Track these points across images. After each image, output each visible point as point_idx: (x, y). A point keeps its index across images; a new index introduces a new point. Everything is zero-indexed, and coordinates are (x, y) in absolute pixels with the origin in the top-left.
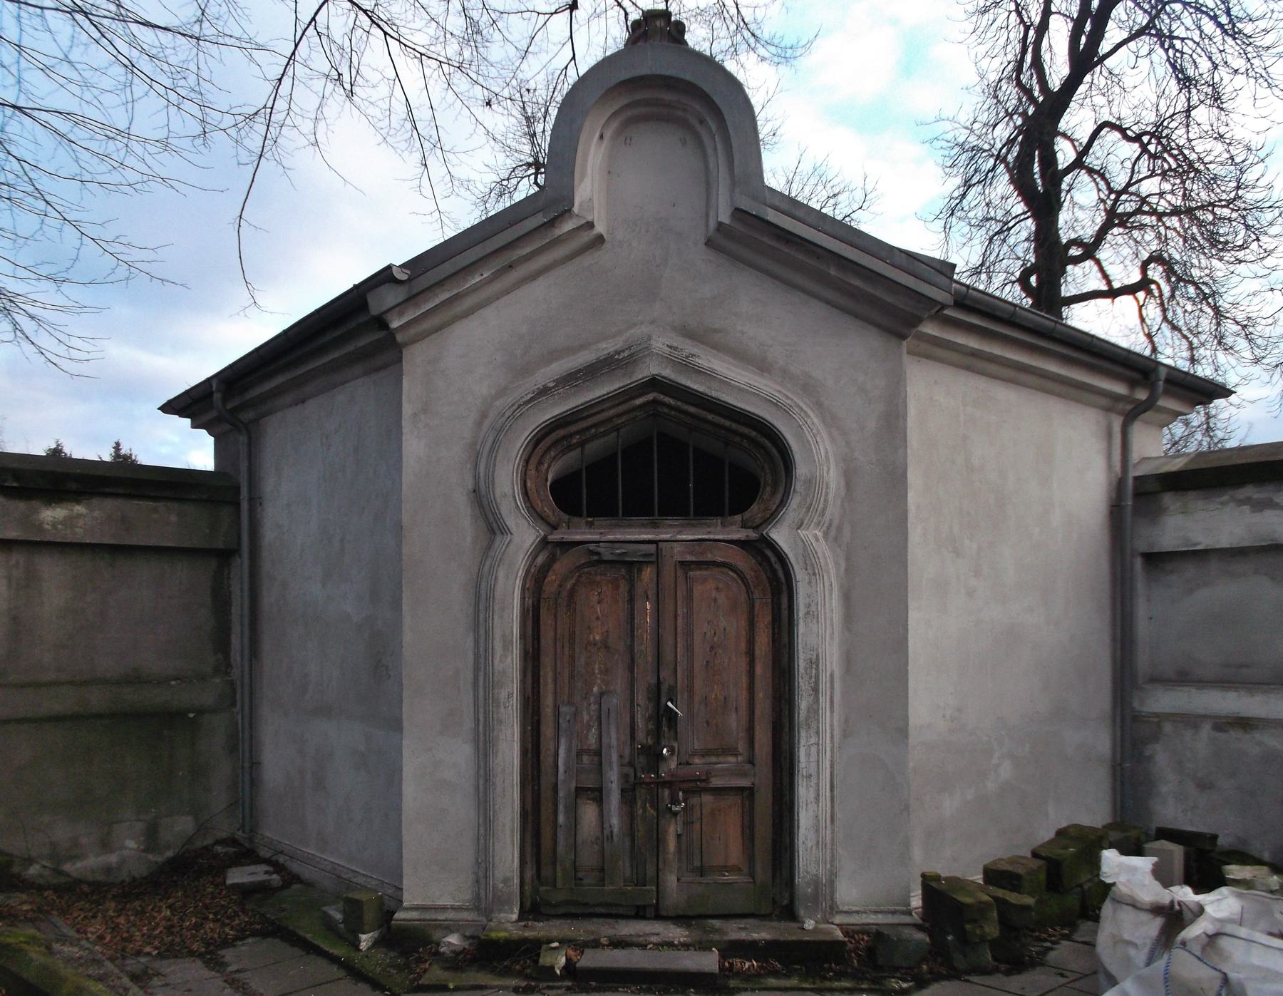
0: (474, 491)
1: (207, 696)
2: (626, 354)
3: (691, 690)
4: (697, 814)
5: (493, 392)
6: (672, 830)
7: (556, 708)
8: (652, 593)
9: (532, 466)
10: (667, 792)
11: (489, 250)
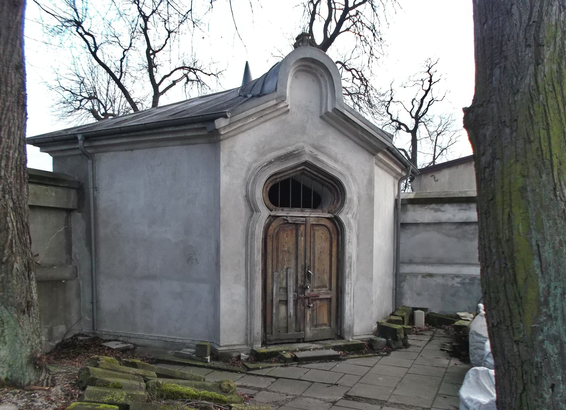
0: (246, 196)
1: (66, 273)
2: (297, 152)
3: (314, 267)
4: (315, 308)
5: (252, 161)
6: (309, 312)
7: (273, 273)
8: (303, 235)
9: (265, 188)
10: (307, 301)
11: (258, 110)
